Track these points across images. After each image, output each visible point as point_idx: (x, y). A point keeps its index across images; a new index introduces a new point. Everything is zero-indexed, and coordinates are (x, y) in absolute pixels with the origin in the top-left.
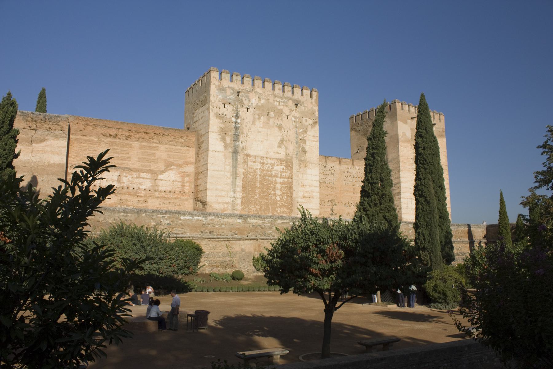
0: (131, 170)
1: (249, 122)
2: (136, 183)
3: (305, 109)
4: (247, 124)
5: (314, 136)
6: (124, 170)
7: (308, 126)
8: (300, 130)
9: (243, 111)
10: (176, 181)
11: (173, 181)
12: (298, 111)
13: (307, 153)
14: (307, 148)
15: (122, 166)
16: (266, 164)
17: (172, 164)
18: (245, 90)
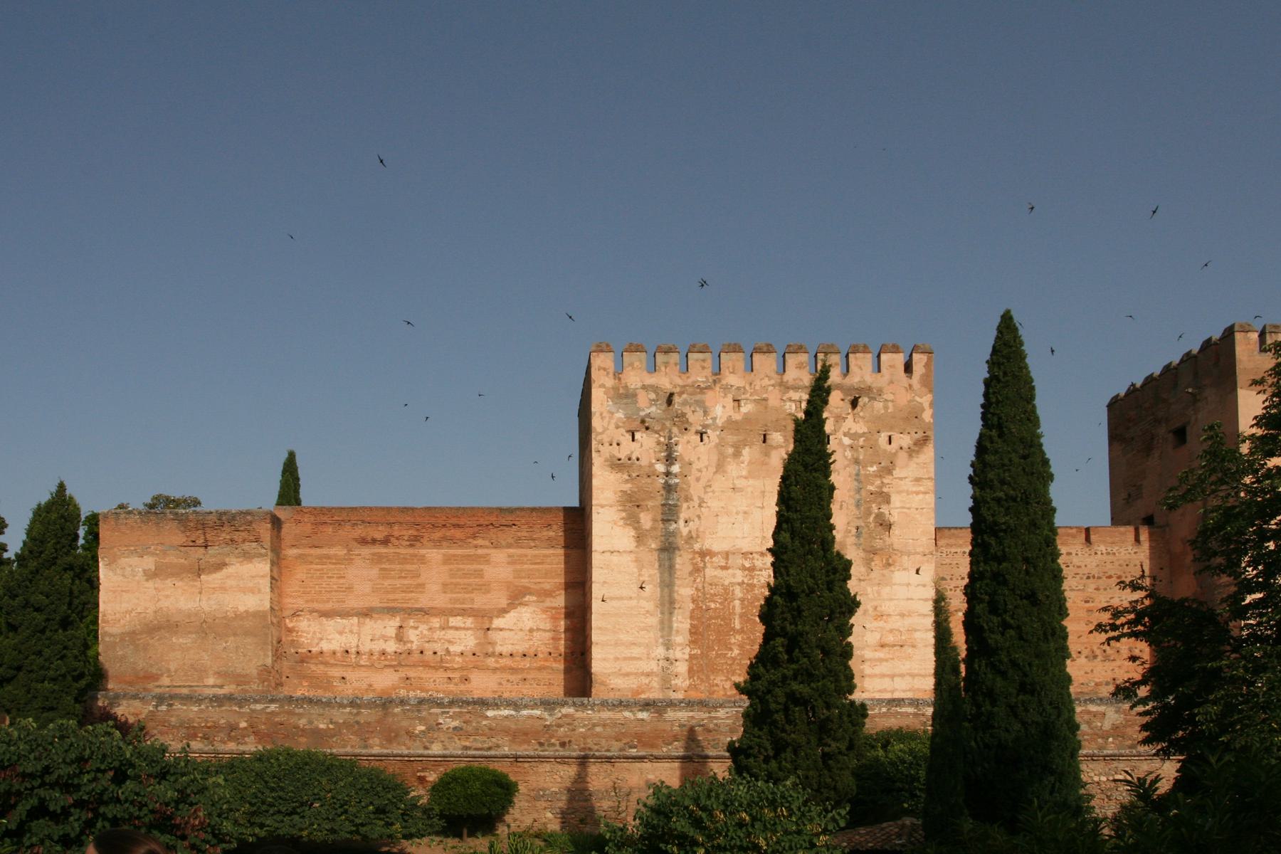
0: (425, 612)
1: (706, 467)
2: (440, 640)
3: (886, 408)
4: (699, 474)
5: (918, 480)
6: (409, 614)
7: (895, 454)
8: (869, 469)
9: (688, 442)
10: (538, 629)
11: (531, 630)
12: (863, 418)
13: (893, 527)
14: (894, 511)
15: (405, 605)
16: (761, 570)
17: (525, 591)
18: (693, 386)
